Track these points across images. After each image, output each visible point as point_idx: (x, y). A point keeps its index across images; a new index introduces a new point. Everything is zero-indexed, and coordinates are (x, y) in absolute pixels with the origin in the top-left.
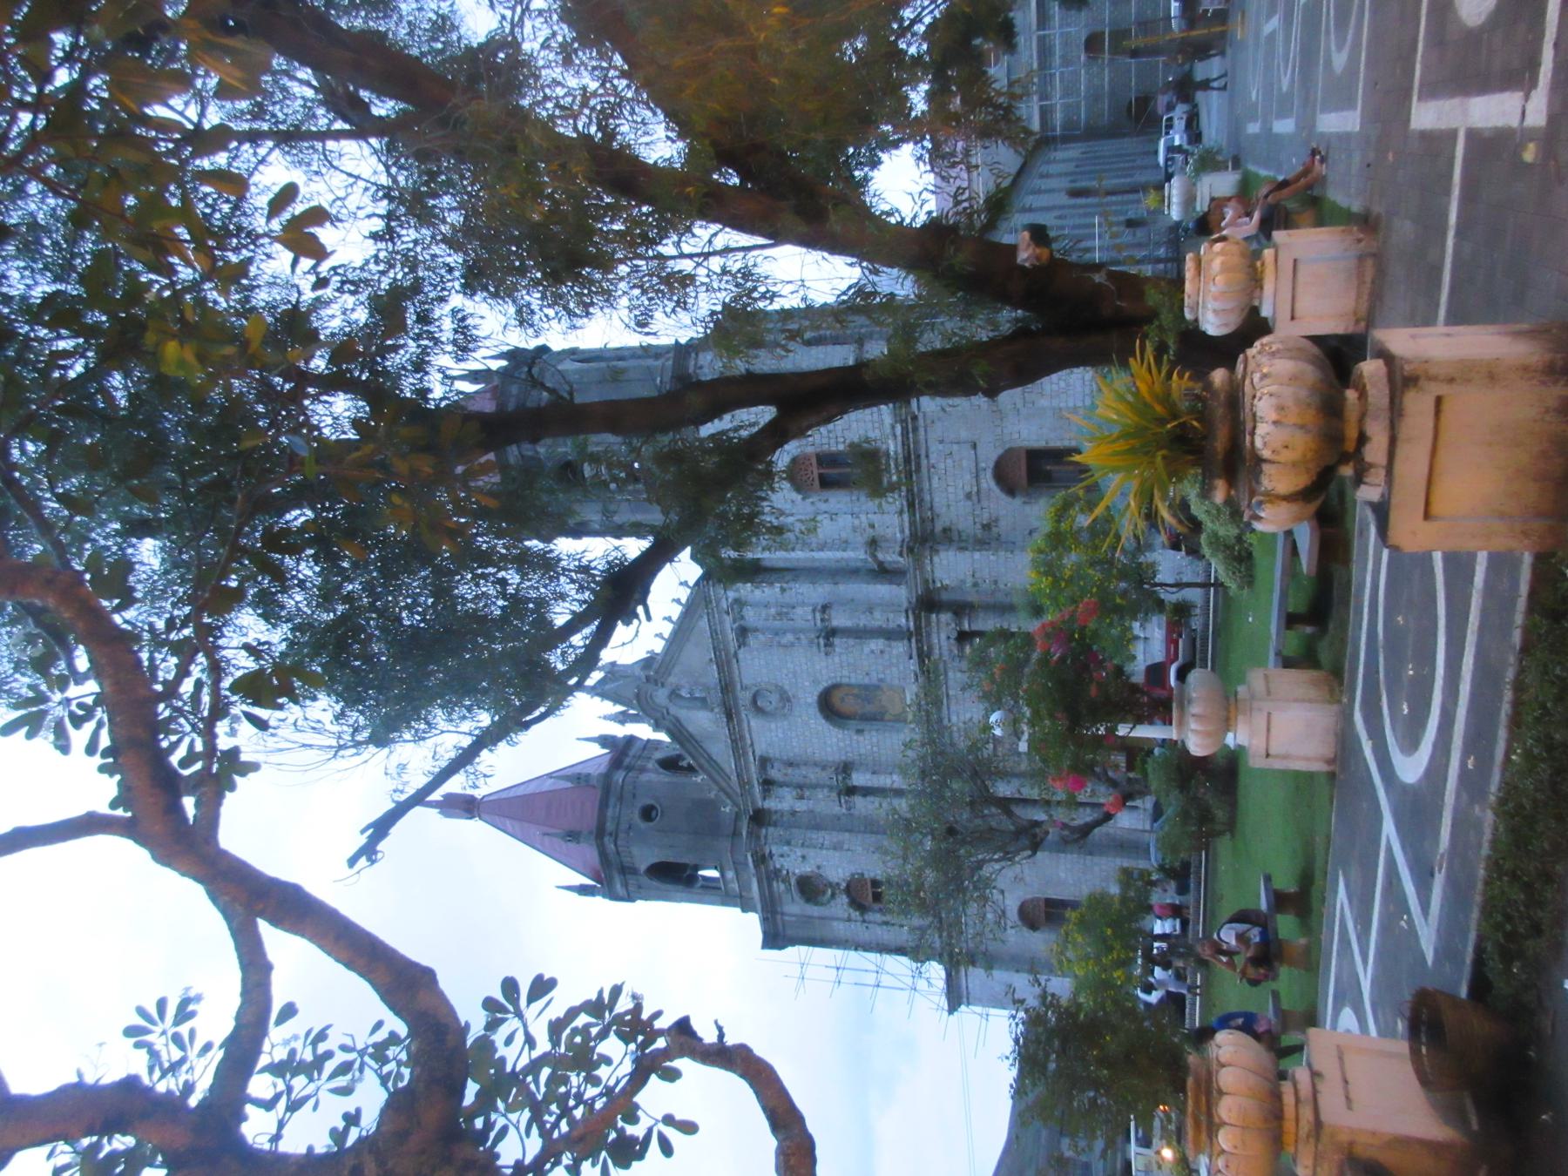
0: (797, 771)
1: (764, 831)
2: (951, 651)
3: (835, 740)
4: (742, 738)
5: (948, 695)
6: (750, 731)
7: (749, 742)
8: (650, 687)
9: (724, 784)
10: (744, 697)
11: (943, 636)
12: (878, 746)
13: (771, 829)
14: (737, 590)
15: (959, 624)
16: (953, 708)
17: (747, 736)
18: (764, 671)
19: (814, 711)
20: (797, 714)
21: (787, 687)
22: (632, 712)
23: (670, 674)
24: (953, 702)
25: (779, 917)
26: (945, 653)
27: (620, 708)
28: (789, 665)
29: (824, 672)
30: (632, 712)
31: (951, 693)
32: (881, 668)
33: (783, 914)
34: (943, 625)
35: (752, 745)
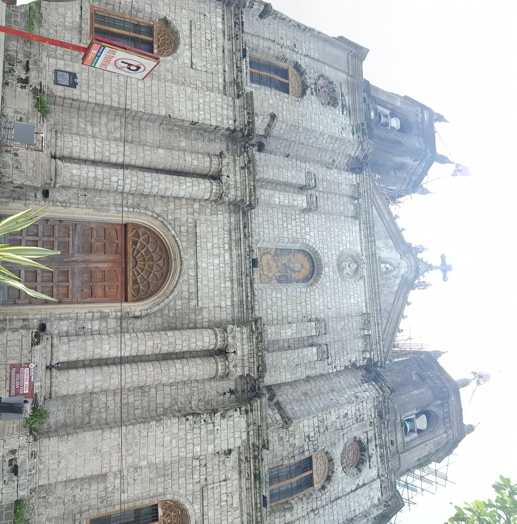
2: (234, 338)
3: (312, 234)
4: (366, 237)
5: (232, 280)
6: (361, 243)
11: (239, 352)
15: (227, 367)
19: (325, 260)
20: (334, 258)
24: (227, 275)
26: (238, 335)
29: (317, 297)
31: (228, 284)
32: (279, 302)
33: (348, 74)
35: (360, 230)
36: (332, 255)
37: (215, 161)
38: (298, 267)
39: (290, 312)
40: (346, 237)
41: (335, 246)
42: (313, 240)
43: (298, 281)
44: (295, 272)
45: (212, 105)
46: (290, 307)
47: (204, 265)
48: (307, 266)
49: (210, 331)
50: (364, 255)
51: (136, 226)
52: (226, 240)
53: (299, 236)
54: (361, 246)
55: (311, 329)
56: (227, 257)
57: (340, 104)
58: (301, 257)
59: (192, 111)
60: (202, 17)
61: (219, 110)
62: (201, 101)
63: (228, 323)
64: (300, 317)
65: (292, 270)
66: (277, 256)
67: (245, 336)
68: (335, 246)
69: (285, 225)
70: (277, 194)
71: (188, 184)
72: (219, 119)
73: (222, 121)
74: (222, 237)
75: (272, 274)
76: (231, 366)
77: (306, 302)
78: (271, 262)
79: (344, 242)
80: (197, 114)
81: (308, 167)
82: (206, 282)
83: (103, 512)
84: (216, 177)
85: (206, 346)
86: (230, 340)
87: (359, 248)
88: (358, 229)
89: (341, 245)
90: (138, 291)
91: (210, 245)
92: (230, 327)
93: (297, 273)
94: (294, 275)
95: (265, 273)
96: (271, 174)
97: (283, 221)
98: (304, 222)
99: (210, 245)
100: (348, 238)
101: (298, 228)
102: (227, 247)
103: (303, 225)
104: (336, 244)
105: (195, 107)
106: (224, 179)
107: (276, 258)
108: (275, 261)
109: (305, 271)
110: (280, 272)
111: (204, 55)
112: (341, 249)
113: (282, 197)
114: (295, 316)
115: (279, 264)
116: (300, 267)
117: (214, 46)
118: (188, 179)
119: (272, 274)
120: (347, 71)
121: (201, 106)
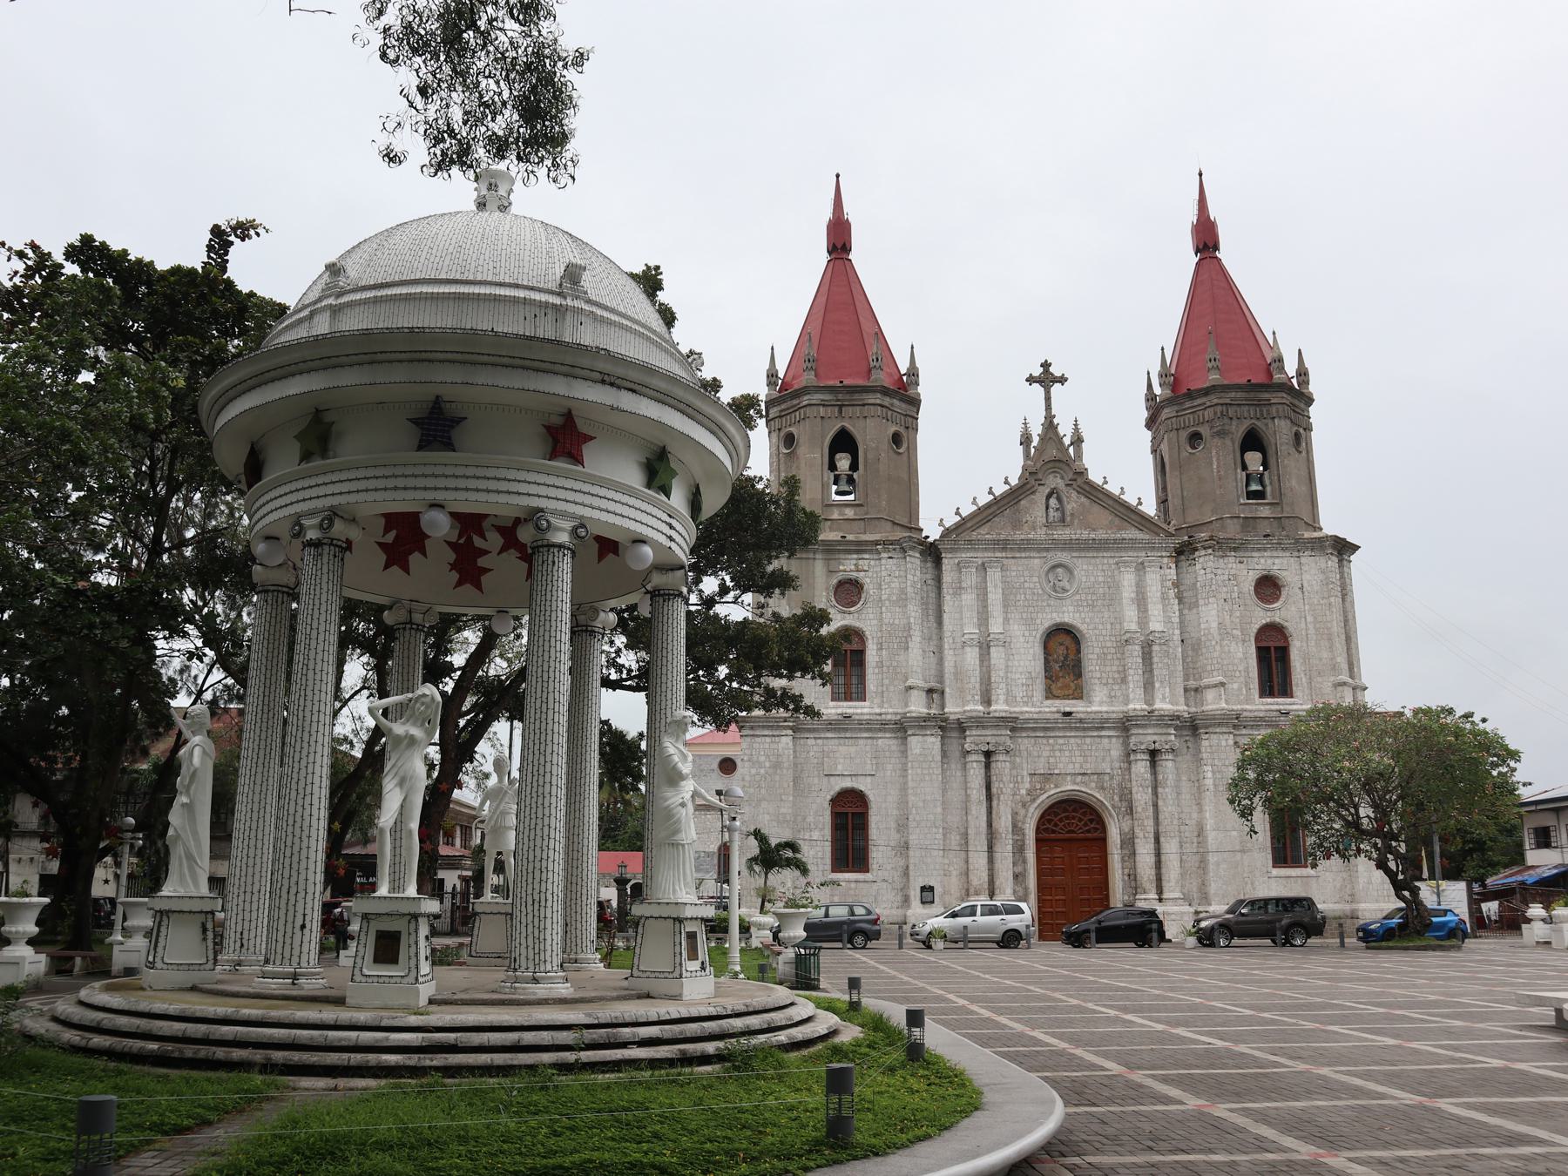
1: (918, 555)
2: (1142, 743)
7: (1018, 555)
8: (1071, 475)
9: (969, 525)
10: (1063, 557)
11: (1155, 738)
13: (918, 561)
16: (1072, 740)
17: (1023, 555)
18: (1092, 579)
21: (1078, 597)
22: (1033, 450)
23: (1078, 492)
25: (811, 556)
27: (1035, 441)
30: (1033, 450)
34: (1163, 738)
36: (1049, 605)
38: (1061, 651)
39: (1114, 668)
42: (1034, 633)
43: (1079, 651)
44: (1067, 654)
46: (1108, 669)
48: (1063, 638)
49: (1133, 765)
50: (1045, 554)
51: (1038, 830)
52: (1045, 741)
54: (1034, 557)
55: (1136, 650)
56: (1061, 741)
57: (855, 574)
58: (1052, 644)
63: (1126, 744)
64: (1119, 655)
65: (1066, 658)
66: (1052, 676)
67: (1141, 731)
75: (1072, 685)
76: (1167, 747)
77: (1103, 648)
78: (1059, 684)
79: (1032, 586)
80: (934, 777)
83: (1269, 850)
84: (988, 754)
85: (1148, 769)
86: (1143, 747)
87: (1037, 561)
88: (1013, 560)
90: (1091, 821)
92: (1132, 746)
94: (1072, 656)
95: (1071, 692)
102: (1051, 741)
104: (1035, 598)
105: (927, 778)
106: (992, 749)
108: (1058, 678)
109: (1068, 641)
110: (1069, 674)
112: (1040, 592)
114: (1117, 663)
115: (1061, 674)
116: (1062, 647)
119: (1072, 685)
120: (811, 561)
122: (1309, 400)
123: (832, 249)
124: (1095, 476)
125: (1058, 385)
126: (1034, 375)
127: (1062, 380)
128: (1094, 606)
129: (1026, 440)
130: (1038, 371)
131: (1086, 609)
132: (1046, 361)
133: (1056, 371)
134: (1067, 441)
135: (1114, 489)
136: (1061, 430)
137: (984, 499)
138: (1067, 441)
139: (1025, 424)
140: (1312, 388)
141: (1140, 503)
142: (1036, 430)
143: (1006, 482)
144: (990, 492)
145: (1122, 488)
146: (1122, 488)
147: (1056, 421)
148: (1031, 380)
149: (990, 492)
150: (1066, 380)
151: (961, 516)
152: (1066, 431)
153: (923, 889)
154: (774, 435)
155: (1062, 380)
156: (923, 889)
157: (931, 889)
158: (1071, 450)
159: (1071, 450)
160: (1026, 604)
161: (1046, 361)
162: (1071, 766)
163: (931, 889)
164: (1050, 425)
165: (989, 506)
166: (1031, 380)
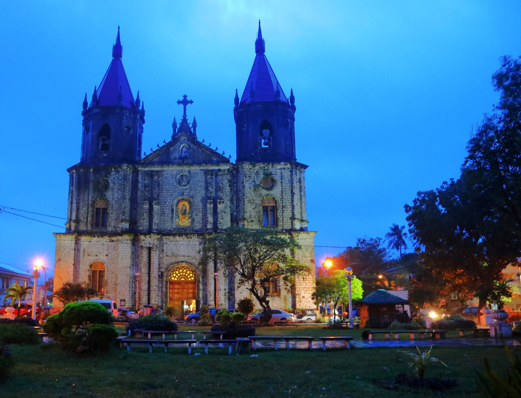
0: (156, 187)
12: (167, 216)
14: (227, 174)
27: (178, 126)
28: (199, 189)
37: (144, 249)
40: (170, 180)
41: (174, 188)
45: (123, 250)
47: (183, 253)
53: (170, 208)
56: (180, 243)
59: (126, 258)
60: (85, 250)
61: (124, 247)
62: (122, 255)
68: (174, 188)
69: (166, 215)
70: (154, 221)
71: (154, 260)
72: (128, 247)
73: (129, 246)
74: (172, 245)
77: (199, 206)
80: (127, 257)
81: (139, 201)
82: (190, 252)
84: (150, 249)
89: (174, 184)
91: (176, 251)
93: (187, 208)
96: (146, 223)
97: (165, 216)
98: (164, 205)
99: (176, 251)
100: (171, 179)
101: (167, 208)
102: (176, 243)
103: (166, 205)
104: (173, 187)
106: (151, 246)
107: (180, 218)
111: (101, 251)
113: (155, 219)
116: (184, 206)
117: (96, 246)
118: (152, 260)
121: (124, 255)
122: (294, 109)
123: (114, 56)
124: (200, 139)
125: (189, 105)
126: (180, 100)
127: (191, 102)
128: (196, 190)
129: (174, 125)
130: (181, 99)
131: (193, 191)
132: (185, 95)
133: (189, 99)
134: (191, 126)
135: (206, 144)
136: (188, 122)
137: (155, 148)
138: (191, 126)
139: (174, 119)
140: (295, 104)
141: (217, 149)
142: (179, 122)
143: (164, 142)
144: (158, 146)
145: (210, 144)
146: (210, 144)
147: (187, 118)
148: (179, 102)
149: (158, 146)
150: (193, 102)
151: (146, 155)
152: (190, 121)
153: (121, 300)
154: (84, 126)
155: (191, 102)
156: (121, 300)
157: (124, 300)
158: (192, 130)
159: (192, 130)
160: (169, 189)
161: (185, 95)
162: (183, 253)
163: (124, 300)
164: (185, 120)
165: (157, 151)
166: (179, 102)
